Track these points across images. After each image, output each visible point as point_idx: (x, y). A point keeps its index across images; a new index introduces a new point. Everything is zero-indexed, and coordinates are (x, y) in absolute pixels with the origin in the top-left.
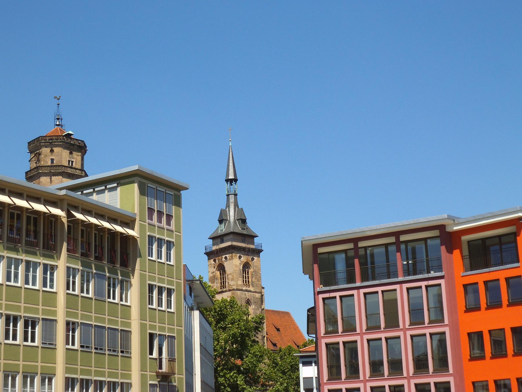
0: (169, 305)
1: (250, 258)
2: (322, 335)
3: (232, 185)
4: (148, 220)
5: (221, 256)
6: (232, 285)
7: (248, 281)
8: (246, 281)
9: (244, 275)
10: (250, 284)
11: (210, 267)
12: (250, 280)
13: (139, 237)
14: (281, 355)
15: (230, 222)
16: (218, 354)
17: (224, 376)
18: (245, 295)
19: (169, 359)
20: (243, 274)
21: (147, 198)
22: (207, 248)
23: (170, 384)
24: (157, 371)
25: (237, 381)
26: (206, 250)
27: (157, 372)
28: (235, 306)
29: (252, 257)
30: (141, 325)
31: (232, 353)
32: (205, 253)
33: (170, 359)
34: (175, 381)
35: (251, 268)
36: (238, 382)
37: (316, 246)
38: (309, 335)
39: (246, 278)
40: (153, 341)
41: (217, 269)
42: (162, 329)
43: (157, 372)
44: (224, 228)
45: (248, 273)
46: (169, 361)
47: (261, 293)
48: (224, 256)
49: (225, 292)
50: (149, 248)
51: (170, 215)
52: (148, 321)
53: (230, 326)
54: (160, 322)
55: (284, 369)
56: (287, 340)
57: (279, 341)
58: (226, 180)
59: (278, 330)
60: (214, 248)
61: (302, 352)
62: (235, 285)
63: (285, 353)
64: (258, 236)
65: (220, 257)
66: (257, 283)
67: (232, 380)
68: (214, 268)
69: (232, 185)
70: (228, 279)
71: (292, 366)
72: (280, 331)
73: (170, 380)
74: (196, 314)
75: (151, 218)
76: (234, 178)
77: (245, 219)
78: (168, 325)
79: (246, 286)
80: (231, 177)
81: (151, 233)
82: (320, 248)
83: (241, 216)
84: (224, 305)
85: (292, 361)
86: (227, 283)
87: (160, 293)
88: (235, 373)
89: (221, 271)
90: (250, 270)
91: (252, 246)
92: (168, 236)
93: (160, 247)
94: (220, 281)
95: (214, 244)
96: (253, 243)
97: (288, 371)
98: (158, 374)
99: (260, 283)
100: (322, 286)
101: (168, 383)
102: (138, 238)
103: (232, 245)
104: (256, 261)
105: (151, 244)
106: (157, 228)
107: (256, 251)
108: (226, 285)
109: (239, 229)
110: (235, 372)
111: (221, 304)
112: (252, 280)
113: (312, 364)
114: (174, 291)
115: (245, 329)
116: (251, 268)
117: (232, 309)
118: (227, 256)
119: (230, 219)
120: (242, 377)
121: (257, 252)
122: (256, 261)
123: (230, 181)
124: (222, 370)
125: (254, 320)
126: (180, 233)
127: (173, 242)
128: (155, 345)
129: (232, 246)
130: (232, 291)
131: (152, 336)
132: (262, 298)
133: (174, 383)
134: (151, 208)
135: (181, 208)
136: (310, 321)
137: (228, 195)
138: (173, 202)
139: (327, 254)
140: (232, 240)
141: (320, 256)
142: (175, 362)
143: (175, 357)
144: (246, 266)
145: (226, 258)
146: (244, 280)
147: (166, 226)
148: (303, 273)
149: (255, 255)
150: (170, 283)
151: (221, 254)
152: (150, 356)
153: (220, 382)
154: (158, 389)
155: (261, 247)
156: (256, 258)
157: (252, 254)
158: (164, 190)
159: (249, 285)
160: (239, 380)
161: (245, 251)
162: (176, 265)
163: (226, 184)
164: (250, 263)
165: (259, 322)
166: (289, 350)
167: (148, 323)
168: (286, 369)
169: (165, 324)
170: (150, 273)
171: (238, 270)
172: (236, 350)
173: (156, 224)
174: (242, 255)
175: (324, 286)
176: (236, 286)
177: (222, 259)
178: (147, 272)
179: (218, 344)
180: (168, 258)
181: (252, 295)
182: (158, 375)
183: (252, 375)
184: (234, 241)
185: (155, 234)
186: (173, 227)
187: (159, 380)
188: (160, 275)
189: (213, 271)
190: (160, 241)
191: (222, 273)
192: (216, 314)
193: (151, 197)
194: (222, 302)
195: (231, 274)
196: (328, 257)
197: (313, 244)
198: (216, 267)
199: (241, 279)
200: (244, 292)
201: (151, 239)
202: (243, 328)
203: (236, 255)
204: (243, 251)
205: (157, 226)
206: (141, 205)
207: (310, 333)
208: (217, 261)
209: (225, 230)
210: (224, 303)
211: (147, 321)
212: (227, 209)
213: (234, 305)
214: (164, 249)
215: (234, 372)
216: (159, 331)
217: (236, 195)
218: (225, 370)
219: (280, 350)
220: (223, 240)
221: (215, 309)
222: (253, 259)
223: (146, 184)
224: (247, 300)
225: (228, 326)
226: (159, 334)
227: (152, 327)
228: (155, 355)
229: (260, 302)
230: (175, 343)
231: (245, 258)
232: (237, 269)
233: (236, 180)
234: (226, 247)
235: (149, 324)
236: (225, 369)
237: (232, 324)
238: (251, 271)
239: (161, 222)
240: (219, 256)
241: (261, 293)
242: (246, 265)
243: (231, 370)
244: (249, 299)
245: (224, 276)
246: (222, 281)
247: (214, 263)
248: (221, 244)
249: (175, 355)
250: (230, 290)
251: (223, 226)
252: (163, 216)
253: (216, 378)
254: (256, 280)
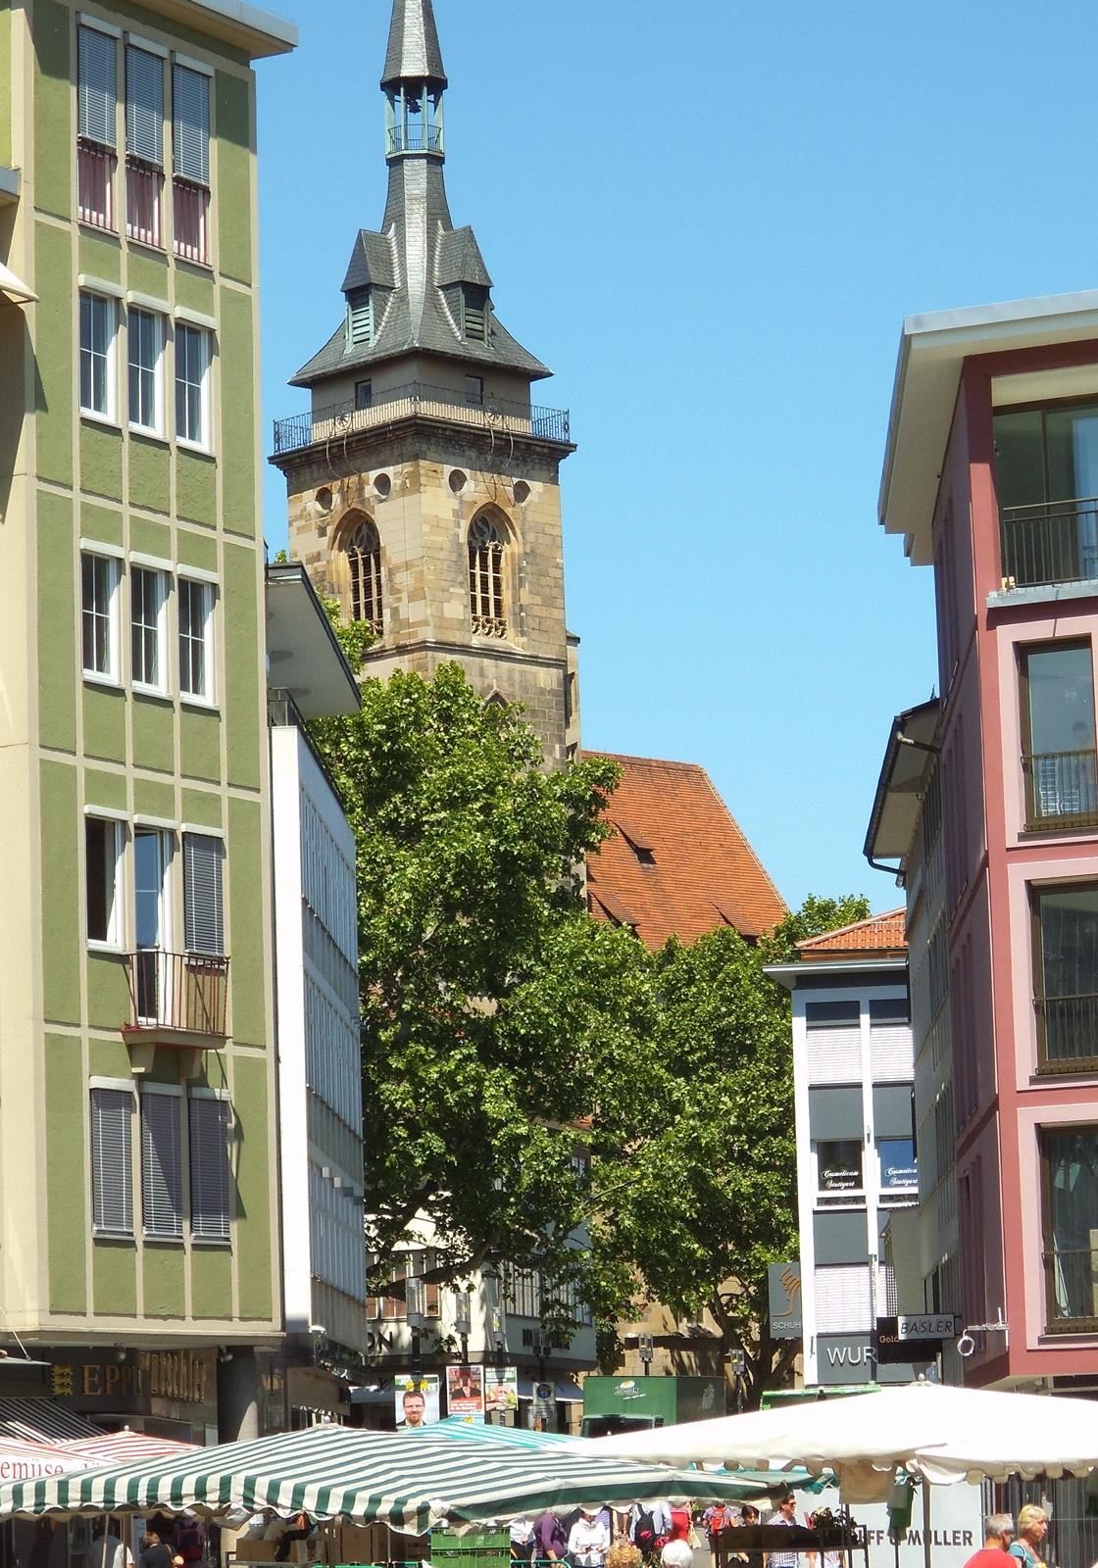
0: (190, 672)
1: (507, 484)
2: (1012, 841)
3: (415, 109)
4: (81, 209)
5: (360, 471)
6: (414, 625)
7: (498, 603)
8: (485, 601)
9: (477, 571)
10: (507, 617)
11: (298, 528)
12: (507, 597)
13: (33, 294)
14: (667, 981)
15: (403, 299)
16: (379, 964)
17: (409, 1074)
18: (482, 674)
19: (193, 963)
20: (472, 566)
21: (74, 90)
22: (282, 430)
23: (197, 1092)
24: (133, 1024)
25: (479, 1098)
26: (277, 440)
27: (128, 1030)
28: (466, 716)
29: (516, 480)
30: (44, 773)
31: (449, 958)
32: (272, 460)
33: (200, 963)
34: (224, 1076)
35: (515, 534)
36: (487, 1107)
37: (980, 369)
38: (875, 861)
39: (485, 590)
40: (108, 858)
41: (335, 538)
42: (154, 796)
43: (128, 1030)
44: (376, 328)
45: (497, 559)
46: (190, 968)
47: (565, 670)
48: (373, 475)
49: (378, 658)
50: (85, 358)
51: (197, 186)
52: (80, 752)
53: (443, 814)
54: (141, 763)
55: (683, 1052)
56: (690, 908)
57: (648, 914)
58: (384, 86)
59: (645, 855)
60: (324, 431)
61: (805, 956)
62: (432, 624)
63: (689, 971)
64: (551, 375)
65: (354, 479)
66: (543, 612)
67: (451, 1098)
68: (322, 532)
69: (415, 109)
70: (394, 591)
71: (720, 1036)
72: (653, 862)
73: (196, 1074)
74: (286, 741)
75: (93, 195)
76: (427, 74)
77: (485, 283)
78: (184, 776)
79: (484, 627)
80: (414, 66)
81: (99, 276)
82: (1001, 379)
83: (463, 269)
84: (409, 704)
85: (724, 1009)
86: (386, 612)
87: (143, 605)
88: (468, 1058)
89: (358, 551)
90: (506, 549)
91: (517, 426)
92: (183, 299)
93: (140, 354)
94: (352, 603)
95: (318, 415)
96: (523, 410)
97: (703, 1061)
98: (133, 1039)
99: (556, 614)
100: (1012, 579)
101: (189, 1087)
102: (30, 300)
103: (415, 417)
104: (536, 499)
105: (93, 337)
106: (125, 250)
107: (539, 449)
108: (381, 623)
109: (451, 335)
110: (470, 1055)
111: (391, 701)
112: (516, 598)
113: (859, 1018)
114: (215, 595)
115: (524, 836)
116: (515, 534)
117: (446, 731)
118: (389, 471)
119: (404, 282)
120: (504, 1079)
121: (539, 454)
122: (536, 499)
123: (409, 90)
124: (399, 1044)
125: (565, 787)
126: (249, 286)
127: (211, 332)
128: (118, 881)
129: (416, 424)
130: (412, 651)
131: (99, 833)
132: (567, 693)
133: (217, 1090)
134: (94, 143)
135: (254, 151)
136: (894, 782)
137: (395, 162)
138: (213, 116)
139: (1038, 413)
140: (421, 393)
141: (1002, 424)
142: (222, 978)
143: (221, 949)
144: (488, 526)
145: (383, 483)
146: (474, 598)
147: (172, 246)
148: (882, 522)
149: (533, 469)
150: (196, 550)
151: (358, 462)
152: (91, 941)
153: (387, 1106)
154: (135, 1118)
155: (566, 428)
156: (536, 487)
157: (518, 465)
158: (163, 52)
159: (501, 623)
160: (493, 1096)
161: (481, 451)
162: (224, 454)
163: (387, 104)
164: (509, 511)
165: (588, 797)
166: (721, 958)
167: (80, 763)
168: (692, 1051)
169: (172, 773)
170: (91, 493)
171: (447, 545)
172: (472, 942)
173: (124, 228)
174: (467, 472)
175: (1022, 582)
176: (439, 627)
177: (361, 489)
178: (77, 486)
179: (376, 912)
180: (186, 416)
181: (517, 676)
182: (135, 1043)
183: (549, 1070)
184: (429, 399)
185: (115, 285)
186: (209, 248)
187: (142, 1070)
188: (142, 507)
189: (314, 550)
190: (142, 320)
191: (360, 562)
192: (367, 753)
193: (98, 85)
194: (396, 688)
195: (407, 566)
196: (1044, 432)
197: (965, 357)
198: (330, 530)
199: (462, 591)
200: (477, 659)
201: (94, 303)
202: (514, 828)
203: (436, 466)
204: (472, 445)
205: (129, 242)
206: (44, 122)
207: (877, 849)
208: (336, 498)
209: (377, 337)
210: (408, 694)
211: (74, 753)
212: (392, 232)
213: (458, 710)
214: (163, 368)
215: (465, 1051)
216: (138, 809)
217: (435, 160)
218: (417, 1042)
219: (669, 955)
220: (368, 391)
221: (360, 726)
222: (522, 491)
223: (72, 14)
224: (492, 700)
225: (433, 817)
226: (137, 827)
227: (106, 787)
228: (119, 936)
229: (556, 712)
230: (220, 874)
231: (482, 487)
232: (442, 539)
233: (436, 84)
234: (385, 426)
235: (87, 770)
236: (418, 1037)
237: (451, 804)
238: (512, 554)
239: (145, 222)
240: (348, 474)
241: (561, 663)
242: (485, 521)
243: (443, 1042)
244: (502, 694)
245: (373, 575)
246: (362, 601)
247: (318, 512)
248: (358, 408)
249: (221, 942)
250: (401, 650)
251: (371, 321)
252: (160, 187)
253: (368, 1087)
254: (538, 600)
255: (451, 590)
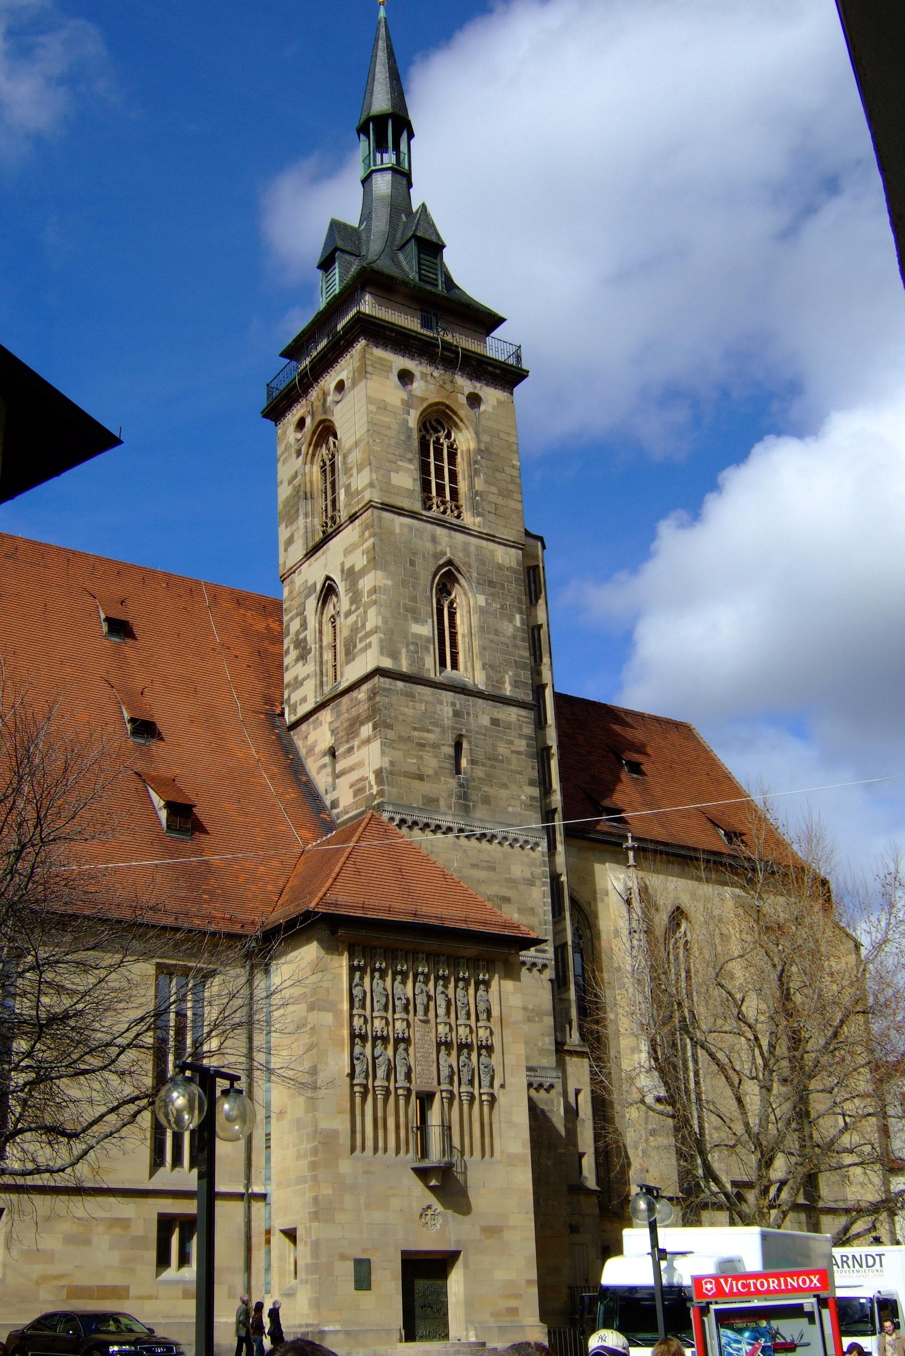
171: (395, 426)
199: (412, 467)
200: (429, 526)
254: (494, 490)
255: (399, 463)
